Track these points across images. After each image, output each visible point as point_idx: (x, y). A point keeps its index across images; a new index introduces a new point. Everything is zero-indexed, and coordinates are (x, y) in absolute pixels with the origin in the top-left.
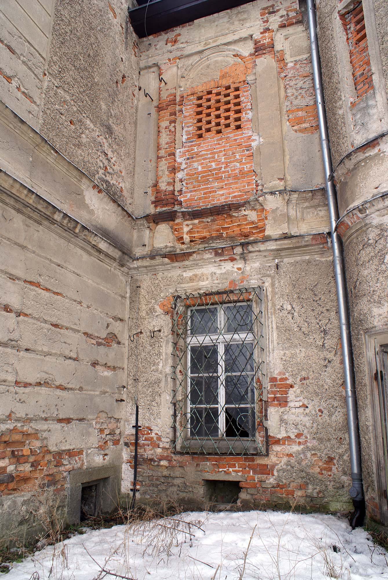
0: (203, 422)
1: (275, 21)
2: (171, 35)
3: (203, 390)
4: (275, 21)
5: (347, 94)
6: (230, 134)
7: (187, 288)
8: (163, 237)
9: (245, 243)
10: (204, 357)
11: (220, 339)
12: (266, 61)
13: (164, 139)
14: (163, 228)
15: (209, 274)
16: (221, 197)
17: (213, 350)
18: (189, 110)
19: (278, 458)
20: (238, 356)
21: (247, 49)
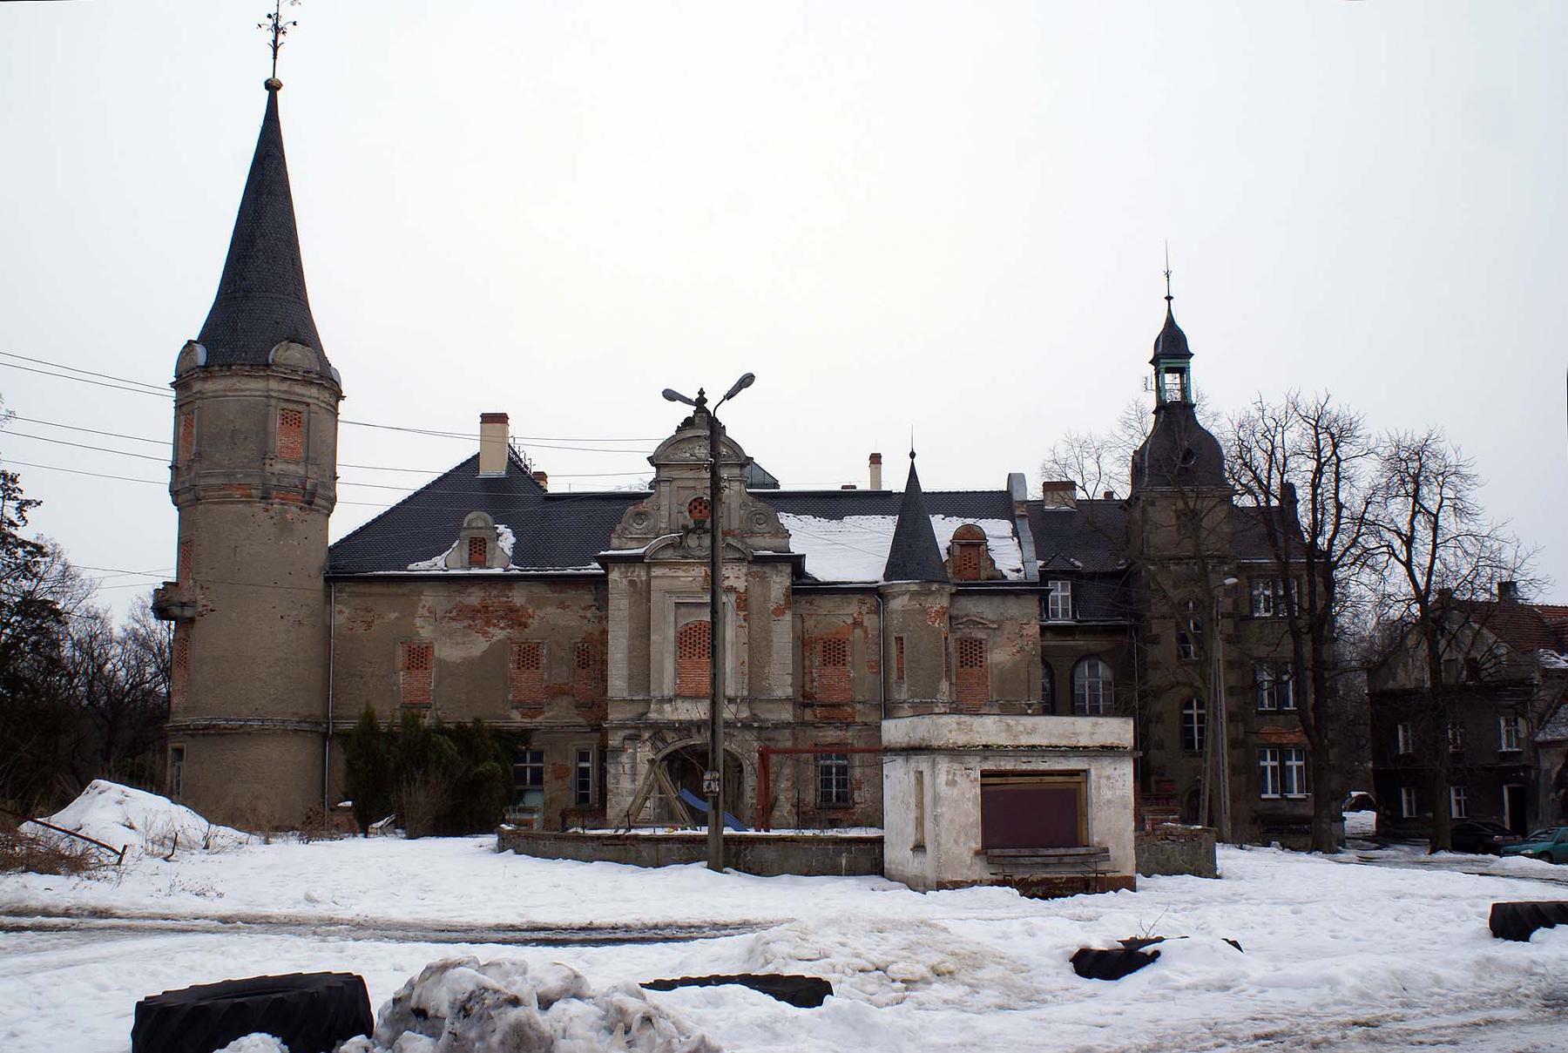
0: (826, 797)
1: (865, 609)
2: (810, 598)
3: (827, 783)
4: (865, 609)
5: (894, 676)
6: (839, 666)
7: (821, 740)
8: (808, 715)
9: (847, 724)
10: (827, 770)
11: (834, 762)
12: (858, 631)
13: (807, 663)
14: (808, 712)
15: (831, 735)
16: (836, 699)
17: (830, 767)
18: (819, 648)
19: (858, 809)
20: (843, 771)
21: (850, 621)
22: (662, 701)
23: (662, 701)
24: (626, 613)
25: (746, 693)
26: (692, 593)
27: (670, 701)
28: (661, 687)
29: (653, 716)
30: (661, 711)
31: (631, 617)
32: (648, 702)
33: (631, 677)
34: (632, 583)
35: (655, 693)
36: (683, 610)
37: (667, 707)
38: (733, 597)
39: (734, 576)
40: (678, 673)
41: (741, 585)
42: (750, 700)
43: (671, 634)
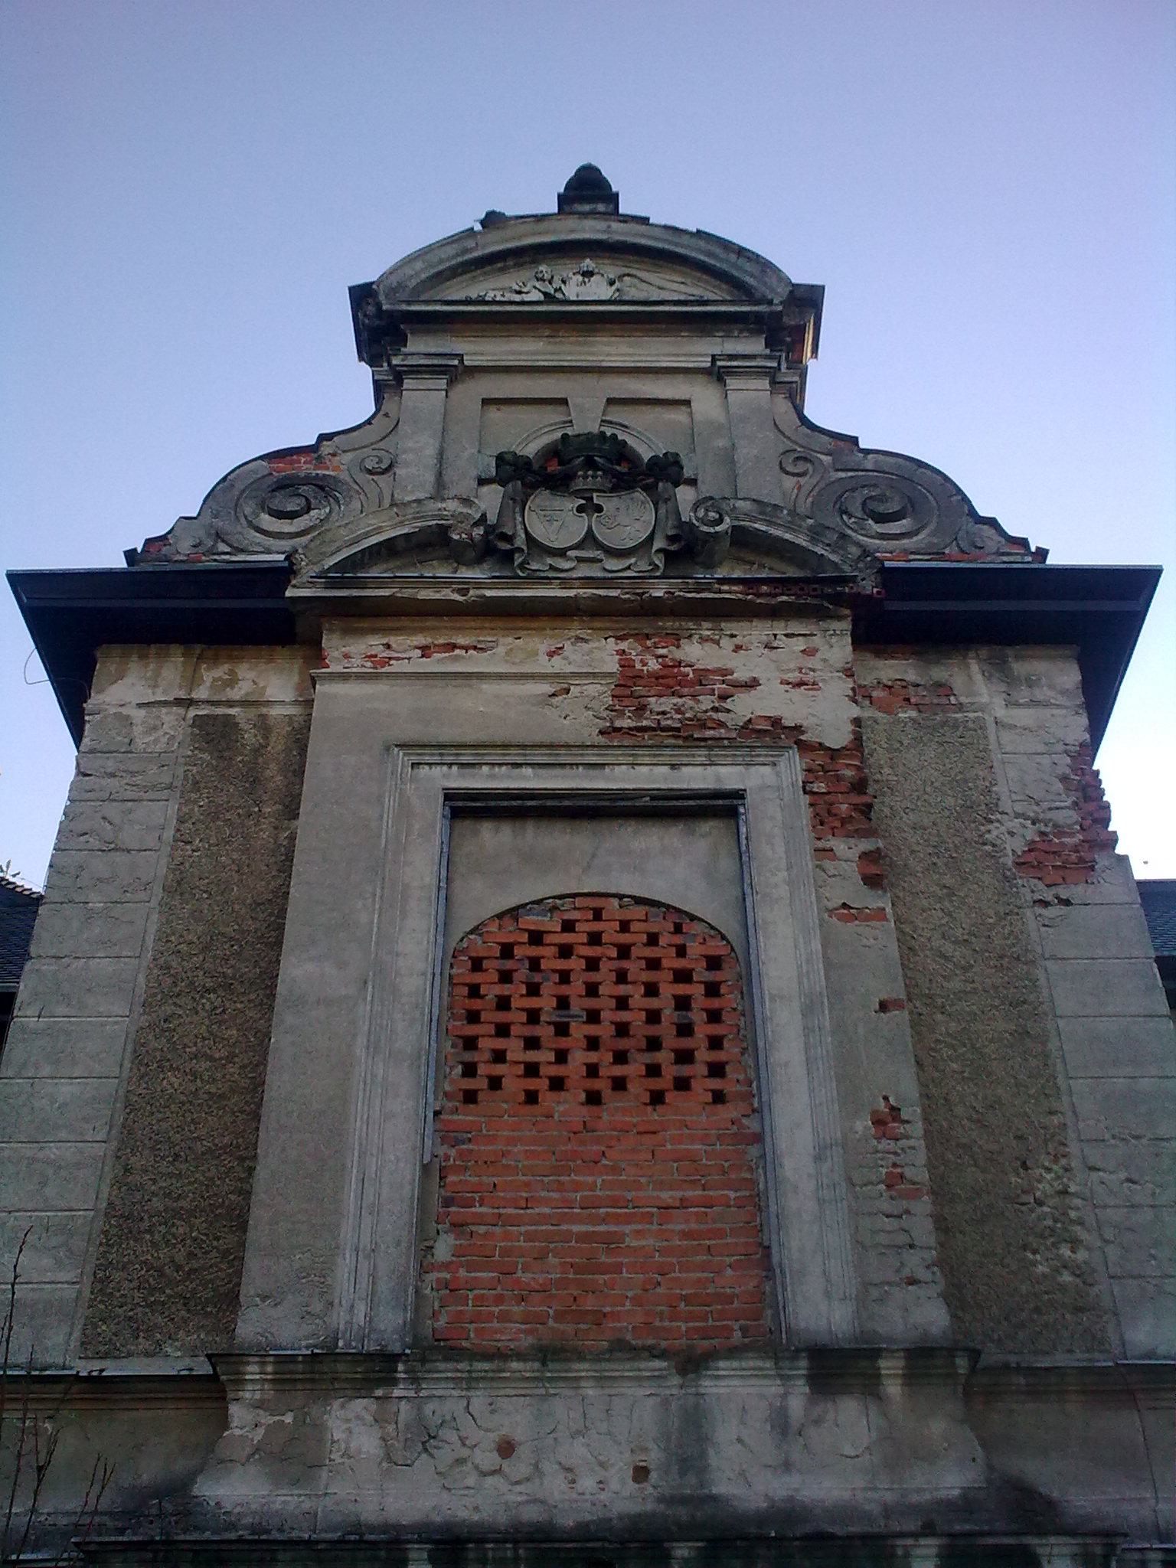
22: (325, 1371)
23: (325, 1371)
24: (156, 866)
25: (931, 1316)
26: (553, 752)
27: (374, 1370)
28: (317, 1278)
29: (237, 1492)
30: (295, 1457)
31: (178, 886)
32: (209, 1391)
33: (123, 1222)
34: (215, 732)
35: (270, 1322)
36: (493, 838)
37: (352, 1427)
38: (791, 767)
39: (795, 676)
40: (445, 1193)
41: (829, 714)
42: (963, 1369)
43: (415, 954)
